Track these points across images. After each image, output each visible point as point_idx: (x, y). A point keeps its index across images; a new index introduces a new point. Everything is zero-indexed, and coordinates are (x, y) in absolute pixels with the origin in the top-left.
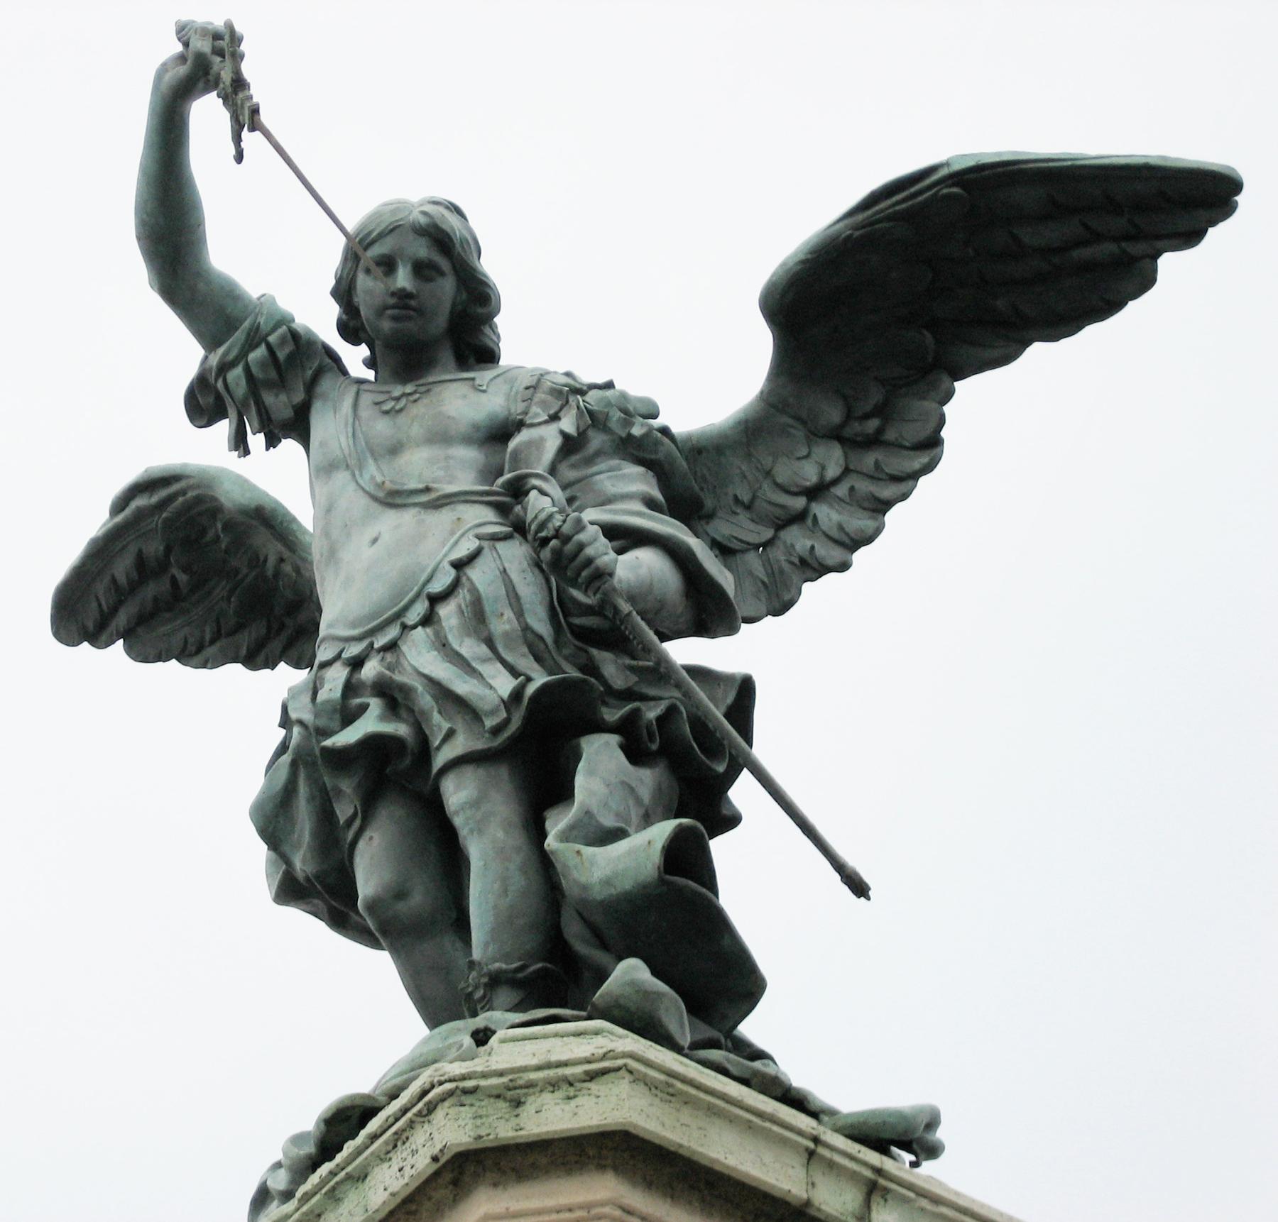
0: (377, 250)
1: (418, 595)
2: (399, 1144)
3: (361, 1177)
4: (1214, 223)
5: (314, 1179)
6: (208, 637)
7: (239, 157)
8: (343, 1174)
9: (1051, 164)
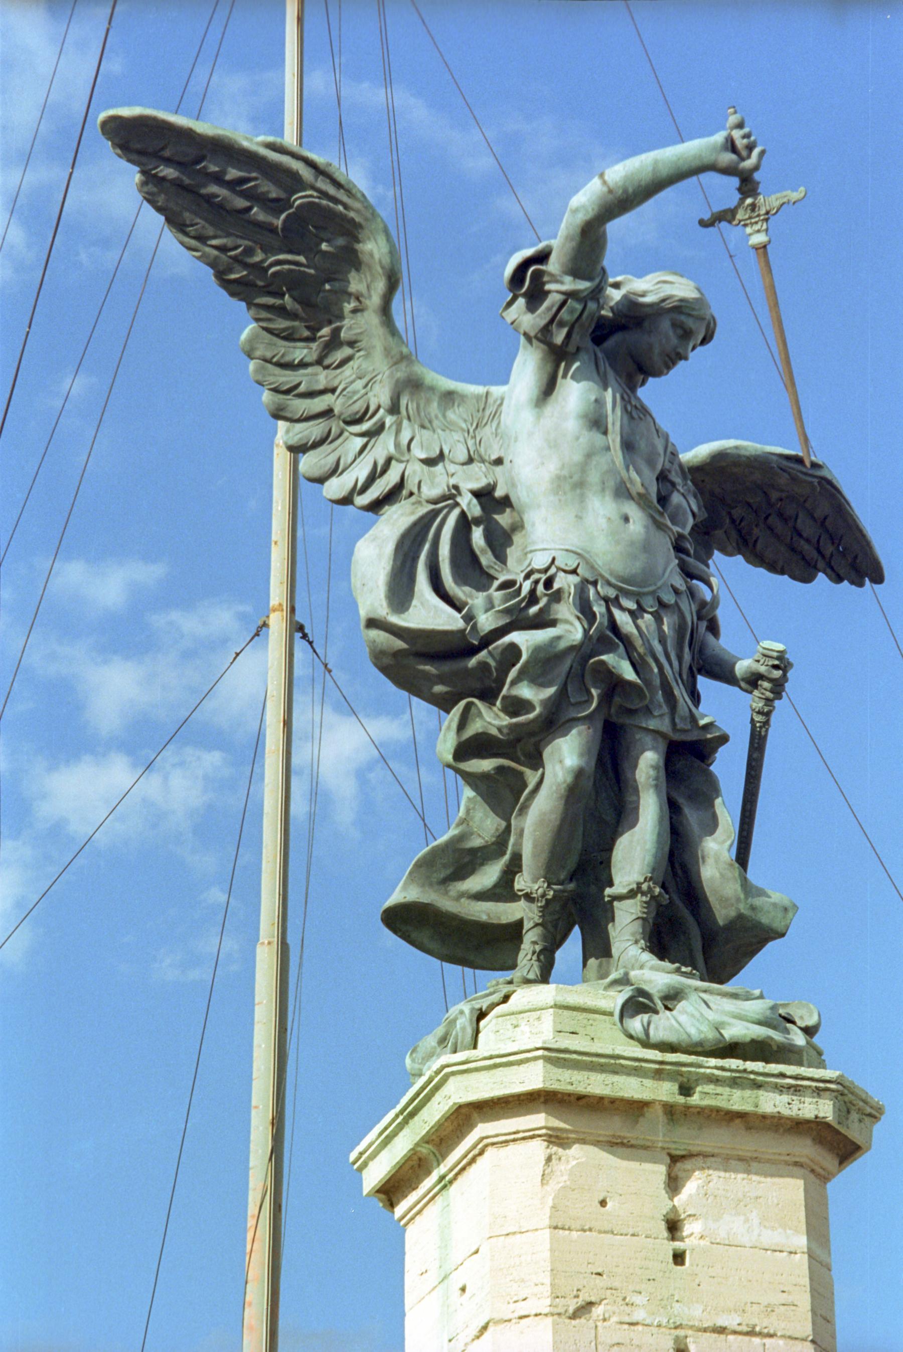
0: (690, 323)
1: (653, 593)
2: (792, 1089)
3: (758, 1086)
4: (852, 582)
5: (734, 1063)
6: (214, 242)
7: (703, 224)
8: (752, 1076)
9: (843, 500)
